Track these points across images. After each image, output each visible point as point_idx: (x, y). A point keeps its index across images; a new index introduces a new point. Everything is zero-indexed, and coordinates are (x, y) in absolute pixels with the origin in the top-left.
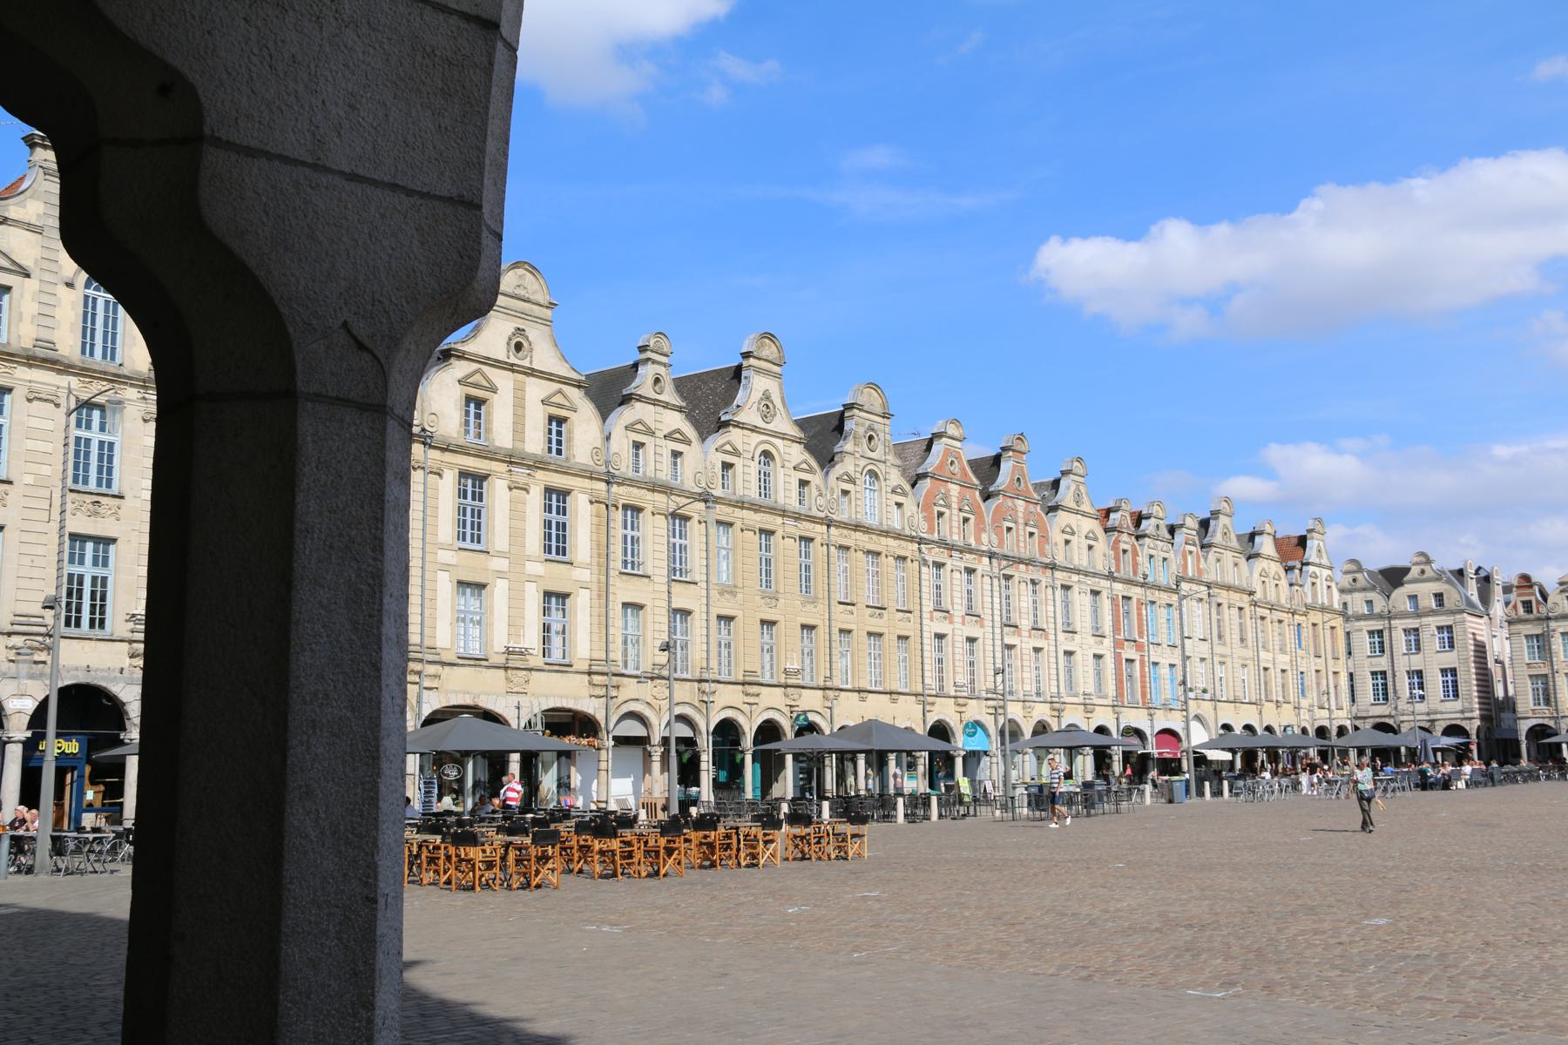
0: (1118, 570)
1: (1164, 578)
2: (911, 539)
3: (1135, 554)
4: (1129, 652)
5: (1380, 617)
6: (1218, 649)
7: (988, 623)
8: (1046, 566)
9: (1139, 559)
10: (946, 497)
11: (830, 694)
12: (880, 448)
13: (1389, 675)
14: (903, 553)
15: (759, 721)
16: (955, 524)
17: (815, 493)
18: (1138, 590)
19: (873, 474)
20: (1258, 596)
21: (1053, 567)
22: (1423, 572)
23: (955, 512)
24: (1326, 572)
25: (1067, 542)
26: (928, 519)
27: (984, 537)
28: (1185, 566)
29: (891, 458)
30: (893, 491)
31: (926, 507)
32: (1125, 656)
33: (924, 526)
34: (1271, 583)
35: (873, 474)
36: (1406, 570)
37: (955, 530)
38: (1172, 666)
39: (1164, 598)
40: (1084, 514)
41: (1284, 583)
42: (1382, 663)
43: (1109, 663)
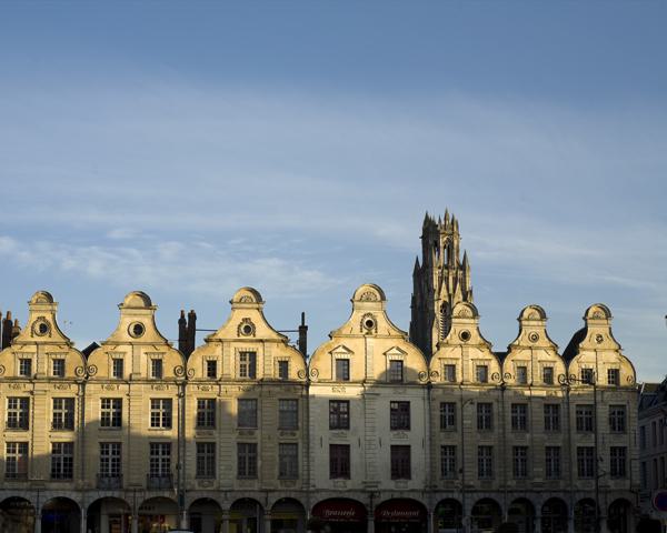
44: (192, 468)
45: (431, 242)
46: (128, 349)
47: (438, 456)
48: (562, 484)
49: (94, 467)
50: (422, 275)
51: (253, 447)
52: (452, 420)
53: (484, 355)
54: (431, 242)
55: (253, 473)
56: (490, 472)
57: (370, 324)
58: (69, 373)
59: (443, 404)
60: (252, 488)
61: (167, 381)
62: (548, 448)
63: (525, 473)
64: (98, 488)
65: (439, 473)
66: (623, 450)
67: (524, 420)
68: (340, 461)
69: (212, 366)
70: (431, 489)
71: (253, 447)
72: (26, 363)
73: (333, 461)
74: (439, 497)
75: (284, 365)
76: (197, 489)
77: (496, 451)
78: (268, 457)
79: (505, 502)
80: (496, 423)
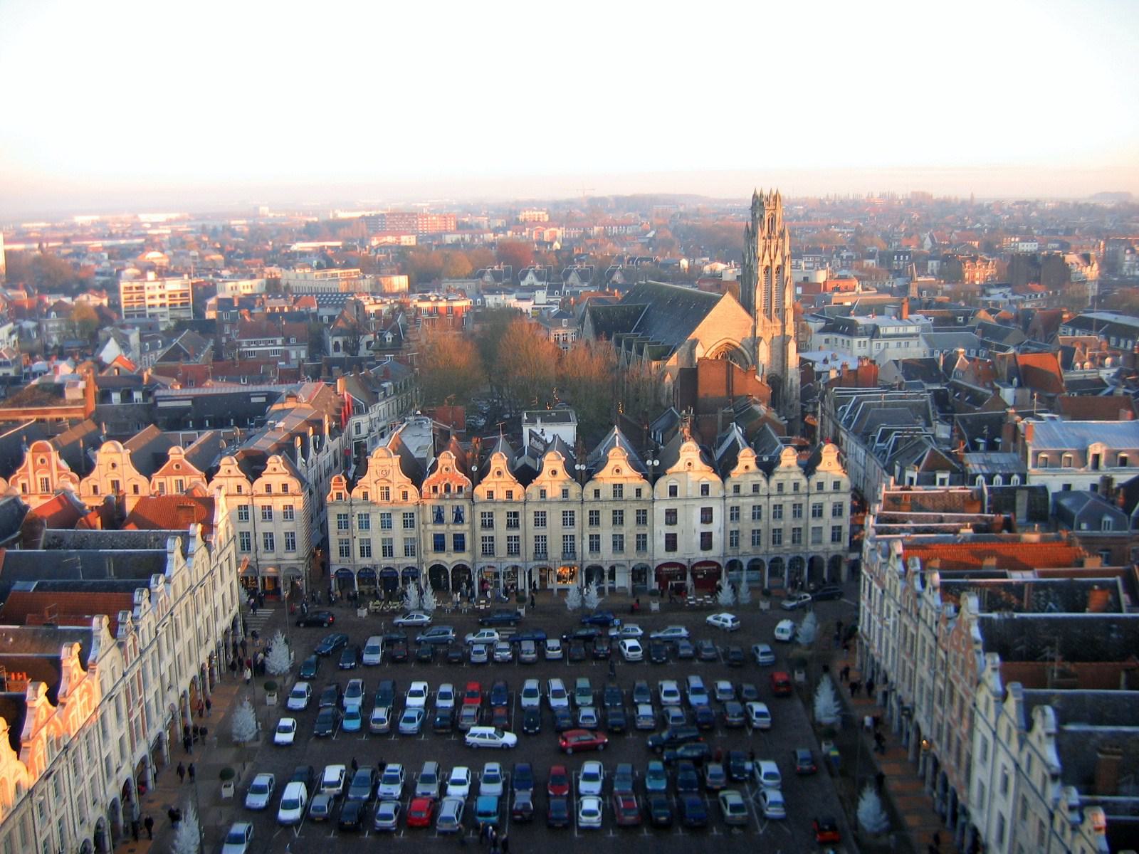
13: (252, 534)
22: (275, 469)
45: (758, 216)
48: (802, 548)
49: (531, 549)
51: (622, 536)
52: (738, 515)
54: (758, 216)
55: (622, 548)
56: (759, 543)
57: (690, 464)
58: (515, 498)
59: (732, 508)
60: (621, 558)
62: (794, 529)
63: (780, 542)
64: (535, 560)
66: (840, 528)
67: (781, 513)
68: (671, 542)
69: (597, 493)
70: (725, 555)
71: (622, 536)
72: (490, 494)
74: (728, 559)
75: (639, 492)
76: (590, 560)
77: (762, 532)
78: (630, 542)
79: (766, 560)
80: (763, 516)
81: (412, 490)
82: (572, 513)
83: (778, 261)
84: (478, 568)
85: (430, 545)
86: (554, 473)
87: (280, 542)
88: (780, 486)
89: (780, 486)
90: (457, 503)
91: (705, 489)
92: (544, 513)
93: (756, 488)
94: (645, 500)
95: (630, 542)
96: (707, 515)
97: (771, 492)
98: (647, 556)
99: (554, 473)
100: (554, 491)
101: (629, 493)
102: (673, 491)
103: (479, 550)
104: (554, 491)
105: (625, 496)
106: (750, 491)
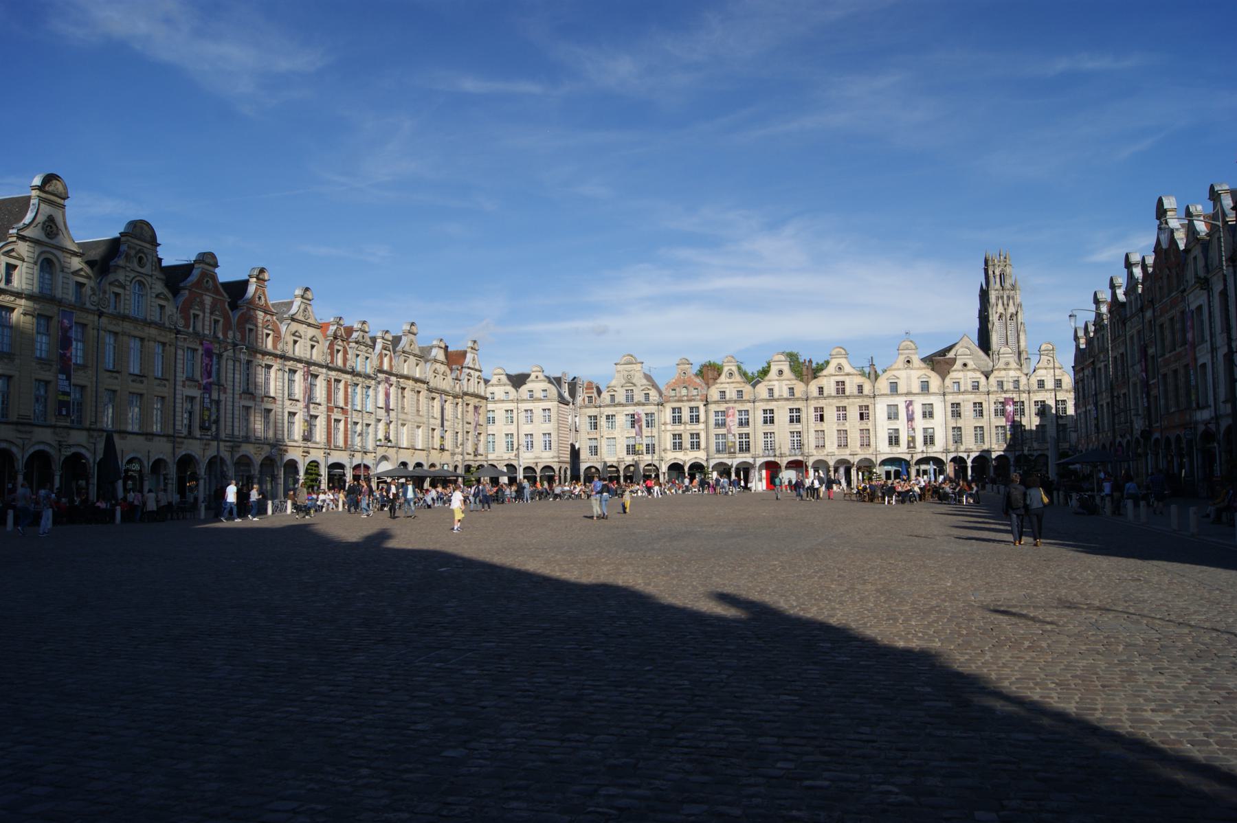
0: (332, 362)
1: (369, 371)
2: (170, 330)
3: (346, 352)
4: (336, 415)
5: (512, 401)
6: (402, 416)
7: (229, 391)
8: (276, 356)
9: (349, 356)
10: (202, 303)
11: (95, 434)
12: (148, 266)
14: (162, 340)
15: (32, 450)
16: (207, 323)
17: (89, 292)
18: (349, 377)
19: (141, 283)
20: (431, 384)
21: (284, 357)
23: (207, 315)
24: (478, 374)
25: (295, 342)
26: (187, 319)
27: (230, 334)
28: (382, 363)
29: (157, 274)
30: (157, 296)
31: (184, 311)
32: (333, 417)
33: (181, 323)
34: (440, 377)
35: (141, 283)
36: (527, 376)
37: (207, 327)
38: (368, 425)
39: (367, 382)
40: (309, 325)
41: (449, 378)
42: (512, 429)
43: (320, 424)
44: (813, 443)
45: (990, 272)
46: (775, 383)
47: (950, 433)
49: (761, 444)
50: (984, 295)
53: (978, 375)
60: (845, 454)
61: (798, 399)
65: (951, 442)
69: (821, 389)
70: (947, 451)
73: (890, 438)
74: (951, 456)
75: (860, 388)
78: (854, 438)
81: (653, 394)
82: (798, 410)
83: (1012, 309)
84: (712, 463)
85: (669, 445)
86: (781, 372)
87: (539, 441)
88: (1001, 384)
89: (1001, 384)
90: (693, 404)
91: (925, 387)
92: (772, 411)
93: (976, 387)
94: (867, 396)
95: (854, 438)
96: (928, 414)
97: (992, 389)
98: (871, 450)
99: (781, 372)
100: (781, 388)
101: (851, 388)
102: (894, 388)
103: (713, 448)
104: (781, 388)
105: (847, 393)
106: (970, 388)
